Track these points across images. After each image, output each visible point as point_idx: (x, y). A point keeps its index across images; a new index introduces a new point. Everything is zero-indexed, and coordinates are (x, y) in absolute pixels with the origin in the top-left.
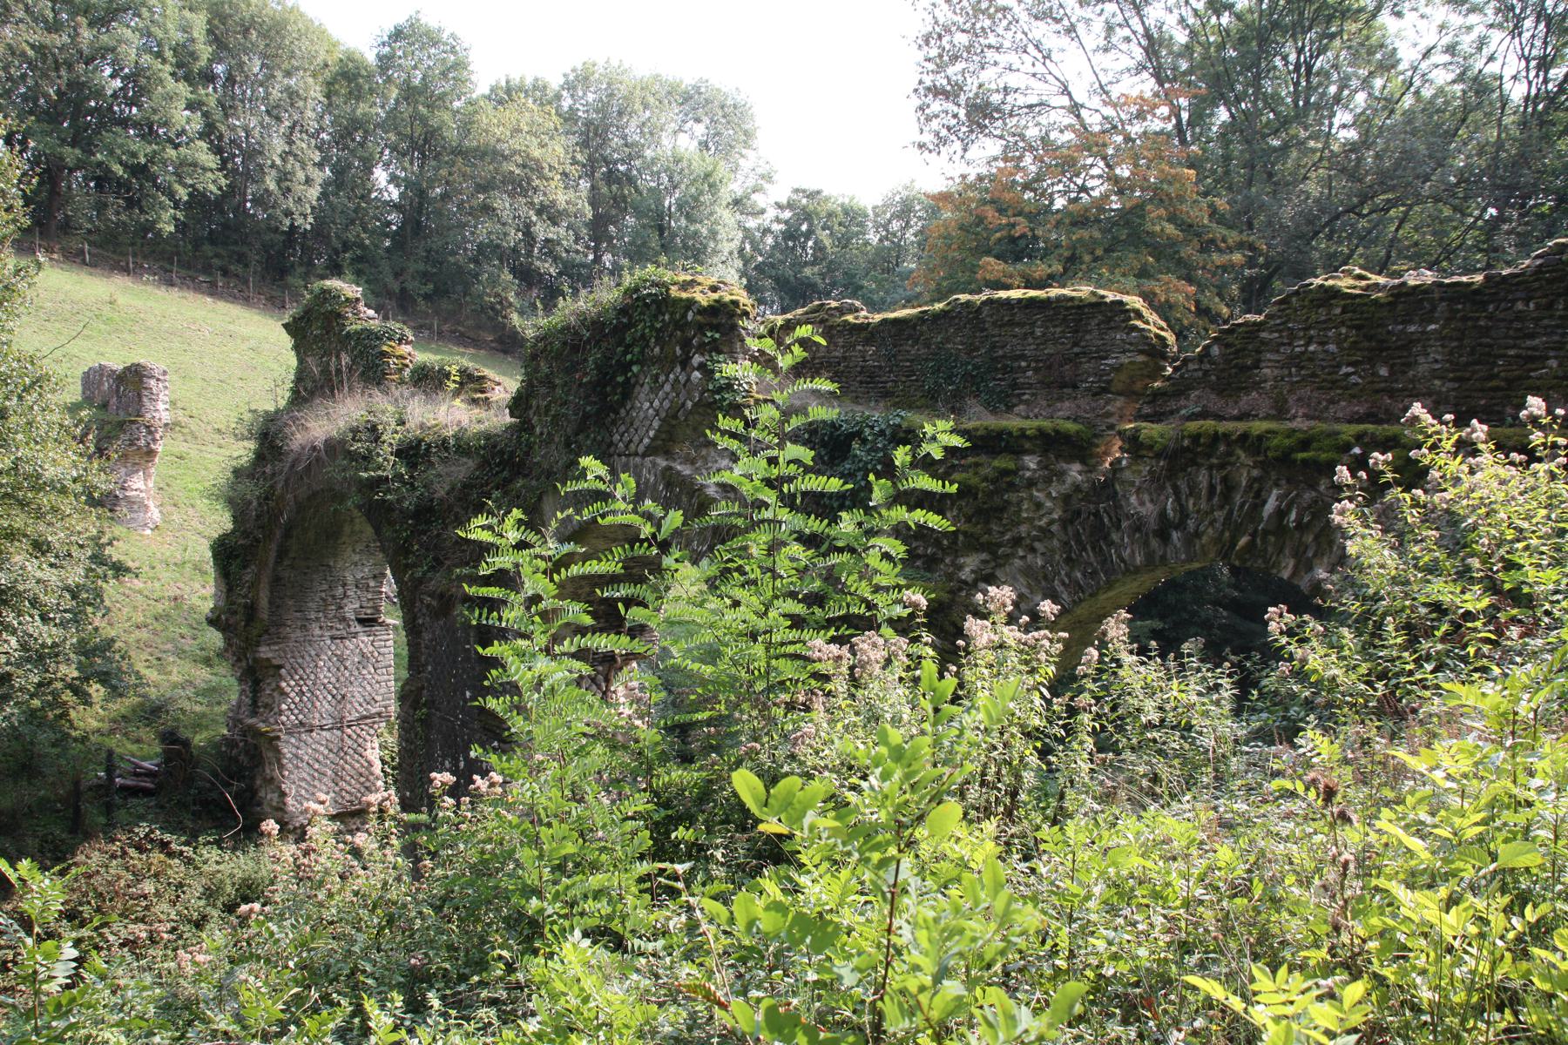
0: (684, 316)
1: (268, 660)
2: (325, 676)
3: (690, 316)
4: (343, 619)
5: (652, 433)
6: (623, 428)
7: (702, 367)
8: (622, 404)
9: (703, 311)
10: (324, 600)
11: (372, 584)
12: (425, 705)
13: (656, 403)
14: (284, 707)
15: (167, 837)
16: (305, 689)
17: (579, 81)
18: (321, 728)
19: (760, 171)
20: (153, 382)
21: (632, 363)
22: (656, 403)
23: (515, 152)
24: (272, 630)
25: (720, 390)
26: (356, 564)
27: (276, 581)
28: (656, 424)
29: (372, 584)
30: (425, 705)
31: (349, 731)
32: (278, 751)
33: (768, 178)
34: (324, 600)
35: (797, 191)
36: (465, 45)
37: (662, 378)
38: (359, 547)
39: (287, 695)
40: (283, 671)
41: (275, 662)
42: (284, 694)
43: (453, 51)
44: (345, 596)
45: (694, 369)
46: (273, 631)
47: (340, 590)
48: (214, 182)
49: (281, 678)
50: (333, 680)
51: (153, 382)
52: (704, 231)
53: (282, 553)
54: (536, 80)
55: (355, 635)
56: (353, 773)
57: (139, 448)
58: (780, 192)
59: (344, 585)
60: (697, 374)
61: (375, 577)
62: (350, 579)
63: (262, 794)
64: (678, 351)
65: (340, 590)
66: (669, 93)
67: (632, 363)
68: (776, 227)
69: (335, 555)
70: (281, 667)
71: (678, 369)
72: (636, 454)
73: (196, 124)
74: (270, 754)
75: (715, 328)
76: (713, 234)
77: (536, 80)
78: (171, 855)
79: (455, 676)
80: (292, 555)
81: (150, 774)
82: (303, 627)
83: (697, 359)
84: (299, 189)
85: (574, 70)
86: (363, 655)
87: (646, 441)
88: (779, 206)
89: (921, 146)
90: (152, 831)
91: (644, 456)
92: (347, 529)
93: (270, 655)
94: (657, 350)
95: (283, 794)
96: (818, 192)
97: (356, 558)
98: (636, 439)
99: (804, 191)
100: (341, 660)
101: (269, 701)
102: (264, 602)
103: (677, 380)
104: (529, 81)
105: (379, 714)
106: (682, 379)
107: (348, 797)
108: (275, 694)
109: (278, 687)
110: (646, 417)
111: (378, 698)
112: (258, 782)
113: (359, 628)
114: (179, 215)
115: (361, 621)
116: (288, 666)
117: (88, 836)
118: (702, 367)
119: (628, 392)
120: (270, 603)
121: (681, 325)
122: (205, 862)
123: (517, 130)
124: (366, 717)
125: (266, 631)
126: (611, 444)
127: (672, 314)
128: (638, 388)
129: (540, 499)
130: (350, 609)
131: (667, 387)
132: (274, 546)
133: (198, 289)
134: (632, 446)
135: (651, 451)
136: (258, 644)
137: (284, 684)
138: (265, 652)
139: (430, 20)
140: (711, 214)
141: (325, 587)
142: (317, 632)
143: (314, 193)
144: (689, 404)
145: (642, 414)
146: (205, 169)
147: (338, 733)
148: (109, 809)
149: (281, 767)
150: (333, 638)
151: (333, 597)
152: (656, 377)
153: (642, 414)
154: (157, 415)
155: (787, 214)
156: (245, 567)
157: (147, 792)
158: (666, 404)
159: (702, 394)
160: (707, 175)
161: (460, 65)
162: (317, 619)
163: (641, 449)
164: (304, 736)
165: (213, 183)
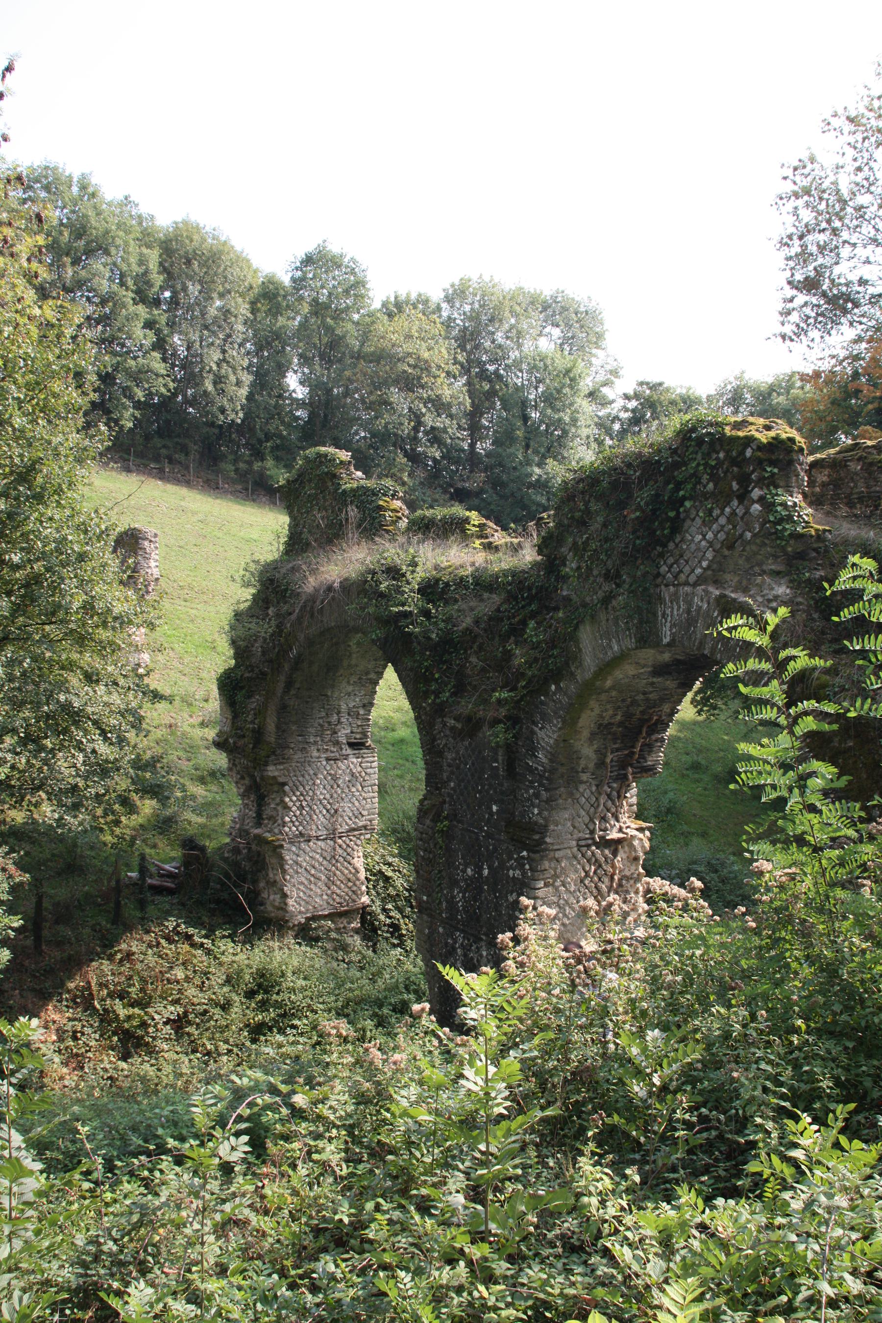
0: (743, 453)
1: (274, 778)
2: (321, 793)
3: (749, 453)
4: (337, 743)
5: (705, 564)
6: (671, 560)
7: (761, 500)
8: (671, 538)
9: (761, 447)
10: (322, 726)
11: (362, 712)
12: (446, 818)
13: (710, 536)
14: (287, 819)
15: (191, 931)
16: (304, 804)
17: (458, 294)
18: (317, 838)
19: (608, 367)
20: (146, 543)
21: (684, 498)
22: (710, 536)
23: (409, 354)
24: (278, 752)
25: (780, 521)
26: (349, 694)
27: (283, 708)
28: (710, 555)
29: (362, 712)
30: (446, 818)
31: (340, 841)
32: (281, 858)
33: (615, 373)
34: (322, 726)
35: (641, 384)
36: (363, 267)
37: (716, 512)
38: (353, 679)
39: (289, 809)
40: (287, 788)
41: (281, 780)
42: (287, 808)
43: (353, 272)
44: (339, 722)
45: (754, 502)
46: (278, 753)
47: (335, 717)
48: (165, 385)
49: (285, 794)
50: (328, 796)
51: (146, 543)
52: (567, 419)
53: (289, 684)
54: (420, 295)
55: (346, 757)
56: (342, 878)
58: (626, 384)
59: (339, 713)
60: (757, 507)
61: (364, 706)
62: (344, 707)
63: (265, 895)
64: (735, 486)
65: (335, 717)
66: (532, 303)
67: (684, 498)
68: (624, 415)
69: (333, 687)
70: (284, 784)
71: (735, 503)
72: (687, 583)
73: (150, 338)
74: (274, 861)
75: (772, 463)
76: (574, 421)
77: (420, 295)
78: (193, 945)
79: (480, 792)
80: (297, 685)
81: (170, 875)
82: (303, 750)
83: (756, 493)
84: (231, 389)
85: (453, 286)
86: (353, 775)
87: (699, 571)
88: (627, 397)
89: (784, 337)
90: (178, 925)
91: (695, 585)
92: (345, 663)
93: (276, 774)
94: (711, 486)
95: (285, 896)
96: (660, 384)
97: (350, 688)
98: (687, 569)
99: (647, 384)
100: (335, 778)
101: (274, 813)
102: (271, 726)
103: (733, 513)
104: (413, 296)
105: (365, 827)
106: (740, 511)
107: (338, 899)
108: (279, 808)
109: (282, 801)
110: (698, 549)
111: (365, 813)
112: (262, 884)
113: (349, 751)
114: (137, 414)
115: (351, 745)
116: (291, 784)
117: (129, 928)
118: (761, 500)
119: (677, 527)
120: (278, 727)
121: (739, 461)
122: (223, 953)
123: (409, 337)
124: (354, 830)
125: (274, 753)
126: (658, 575)
127: (727, 452)
128: (688, 522)
129: (576, 628)
130: (343, 734)
131: (722, 521)
132: (282, 678)
133: (150, 474)
134: (682, 577)
135: (701, 580)
136: (266, 764)
137: (287, 799)
138: (272, 771)
139: (334, 248)
140: (572, 404)
141: (323, 714)
142: (315, 754)
143: (244, 392)
144: (748, 535)
145: (693, 546)
146: (157, 375)
147: (331, 843)
148: (142, 905)
149: (284, 872)
151: (329, 723)
152: (710, 512)
153: (693, 546)
154: (149, 571)
155: (633, 404)
156: (249, 697)
157: (170, 892)
158: (721, 536)
159: (762, 525)
160: (568, 371)
161: (360, 283)
162: (316, 743)
163: (692, 579)
165: (162, 386)
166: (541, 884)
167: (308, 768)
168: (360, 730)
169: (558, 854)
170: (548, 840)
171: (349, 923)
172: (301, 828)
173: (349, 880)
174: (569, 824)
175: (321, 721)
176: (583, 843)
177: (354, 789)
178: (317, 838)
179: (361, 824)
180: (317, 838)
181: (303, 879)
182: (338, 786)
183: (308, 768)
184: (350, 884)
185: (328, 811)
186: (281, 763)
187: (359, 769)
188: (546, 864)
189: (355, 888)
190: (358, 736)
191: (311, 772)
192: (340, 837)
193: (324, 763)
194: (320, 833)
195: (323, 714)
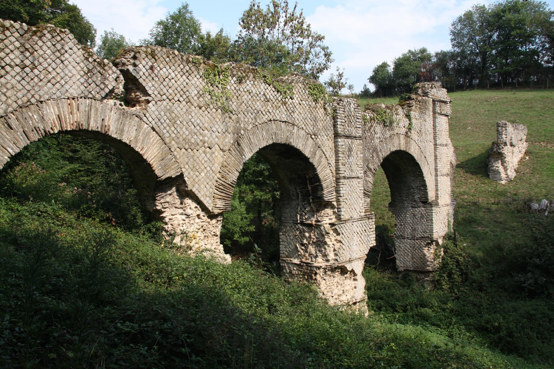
2: (409, 220)
4: (415, 201)
29: (422, 188)
57: (494, 152)
62: (414, 186)
65: (412, 190)
97: (413, 178)
100: (415, 215)
111: (428, 231)
113: (421, 204)
115: (423, 202)
130: (417, 197)
142: (407, 205)
150: (412, 207)
154: (502, 140)
162: (406, 200)
164: (402, 240)
166: (281, 234)
167: (403, 210)
168: (424, 196)
169: (286, 224)
170: (283, 219)
171: (425, 277)
172: (401, 233)
173: (421, 258)
174: (289, 214)
175: (407, 191)
176: (295, 222)
177: (422, 221)
178: (408, 238)
179: (426, 235)
180: (408, 238)
181: (402, 253)
182: (416, 218)
183: (403, 210)
184: (421, 260)
185: (412, 228)
186: (393, 207)
187: (425, 212)
188: (283, 227)
189: (423, 262)
190: (424, 199)
191: (405, 212)
192: (417, 240)
193: (410, 208)
194: (409, 237)
195: (407, 189)
